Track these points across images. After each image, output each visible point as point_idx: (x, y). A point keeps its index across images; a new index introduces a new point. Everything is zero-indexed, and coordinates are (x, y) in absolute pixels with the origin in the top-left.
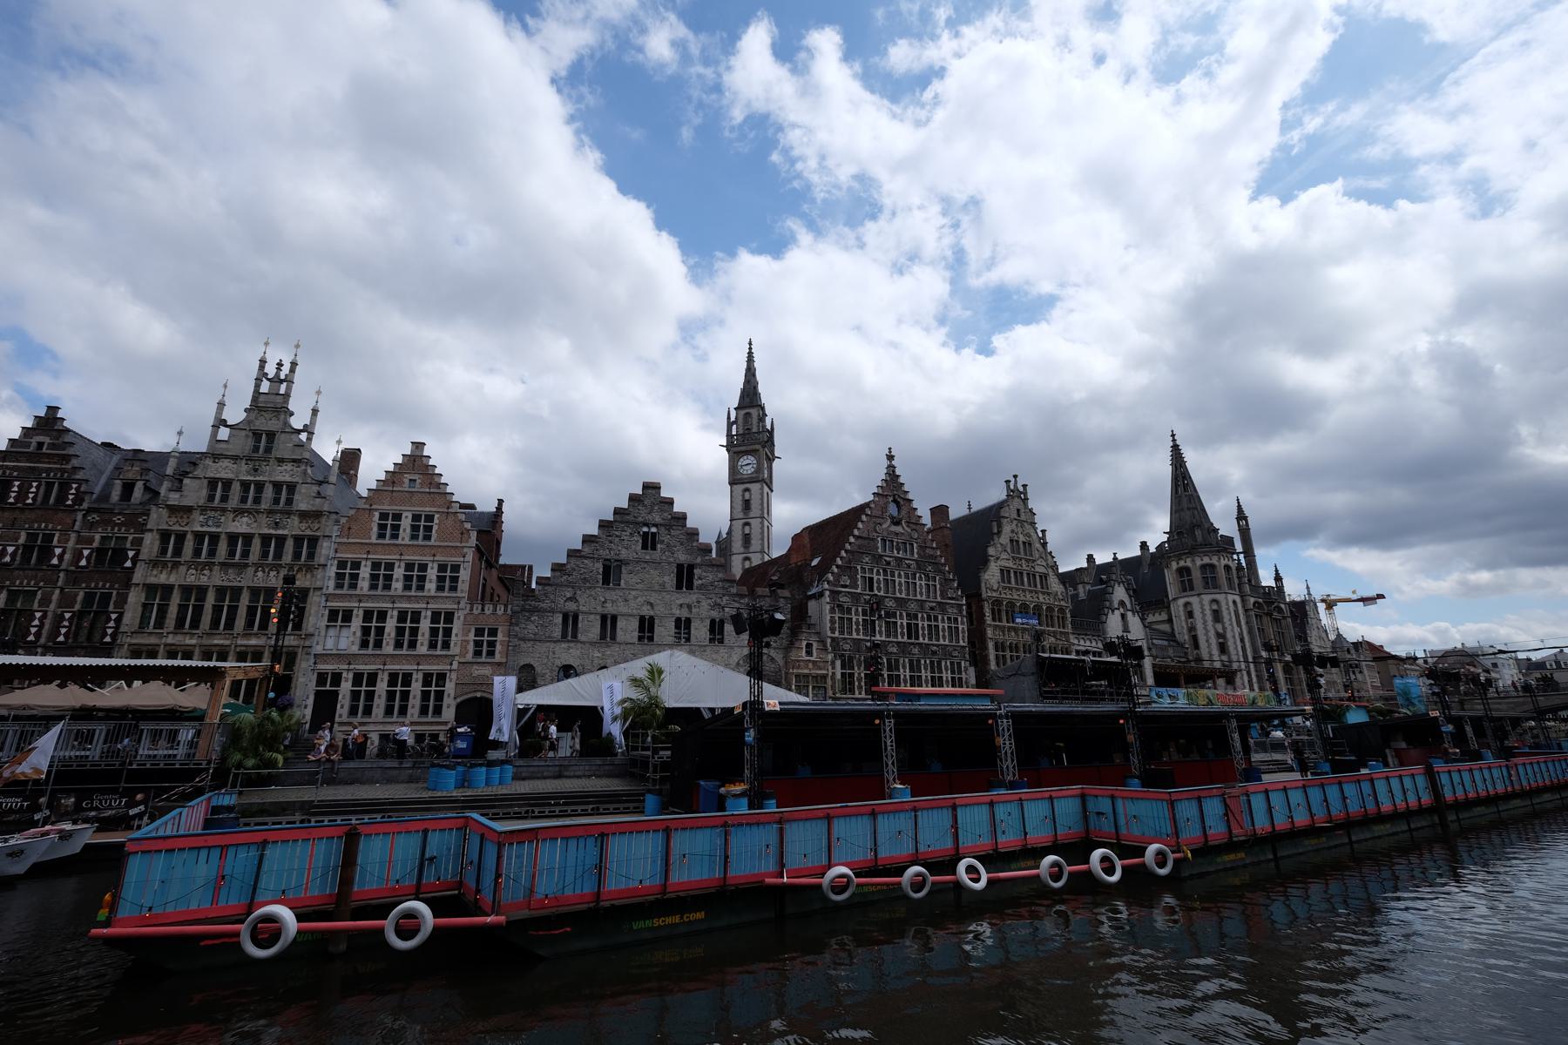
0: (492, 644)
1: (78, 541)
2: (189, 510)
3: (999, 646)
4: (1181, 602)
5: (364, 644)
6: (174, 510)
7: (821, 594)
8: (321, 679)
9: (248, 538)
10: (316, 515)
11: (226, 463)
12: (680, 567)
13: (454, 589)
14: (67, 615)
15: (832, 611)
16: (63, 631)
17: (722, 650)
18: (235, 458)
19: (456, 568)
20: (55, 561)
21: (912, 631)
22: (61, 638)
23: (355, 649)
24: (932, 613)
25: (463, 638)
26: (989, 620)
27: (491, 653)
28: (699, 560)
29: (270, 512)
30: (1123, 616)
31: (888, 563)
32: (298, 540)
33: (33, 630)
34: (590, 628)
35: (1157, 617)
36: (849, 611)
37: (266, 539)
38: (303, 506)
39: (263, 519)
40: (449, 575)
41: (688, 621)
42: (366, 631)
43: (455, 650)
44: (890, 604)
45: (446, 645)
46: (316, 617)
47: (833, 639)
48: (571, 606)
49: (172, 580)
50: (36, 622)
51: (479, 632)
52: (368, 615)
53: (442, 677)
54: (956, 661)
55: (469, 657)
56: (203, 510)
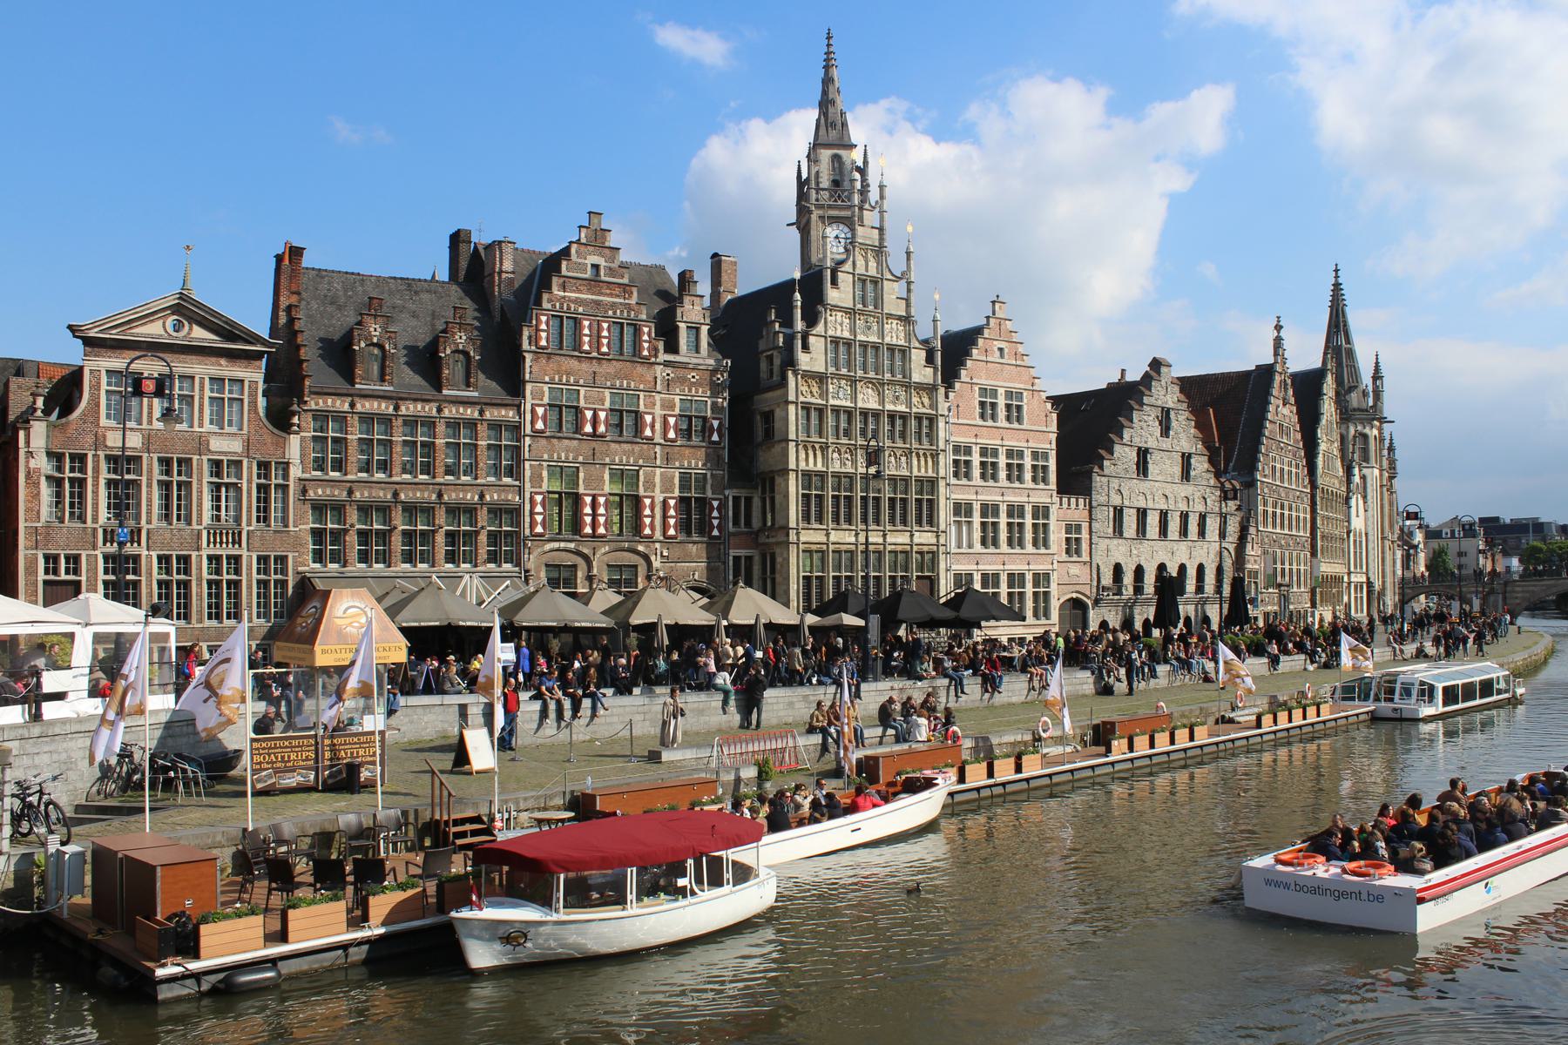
1: (663, 407)
2: (821, 378)
6: (808, 375)
9: (877, 415)
10: (931, 389)
13: (1045, 480)
14: (672, 502)
16: (672, 521)
19: (1046, 456)
20: (648, 432)
22: (672, 532)
25: (1057, 535)
27: (1078, 552)
29: (890, 382)
32: (919, 418)
33: (647, 521)
37: (892, 416)
38: (916, 378)
43: (1054, 548)
45: (1046, 545)
46: (944, 514)
49: (820, 467)
50: (647, 512)
53: (1047, 576)
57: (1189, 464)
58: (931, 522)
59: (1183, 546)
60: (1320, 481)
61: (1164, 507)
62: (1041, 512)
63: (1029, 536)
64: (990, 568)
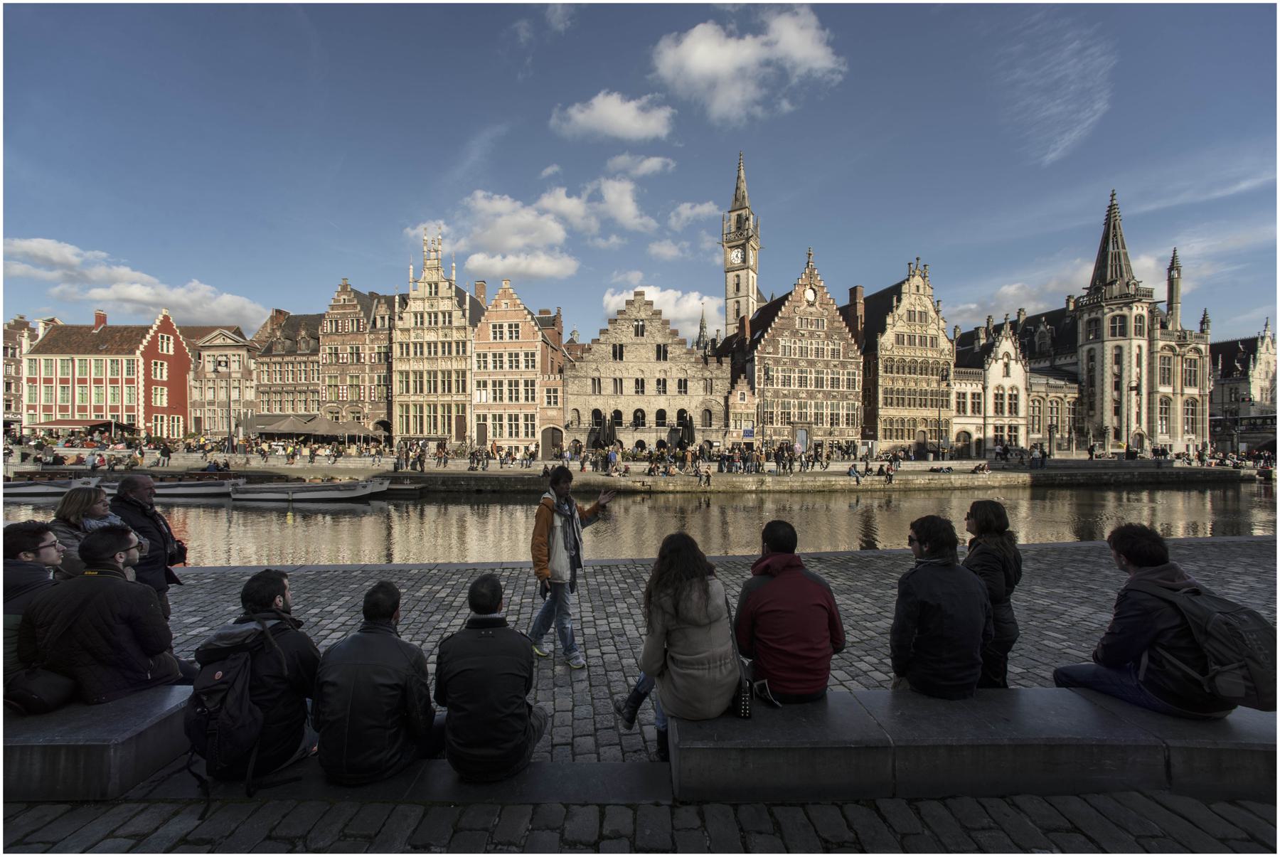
0: (556, 397)
2: (408, 330)
3: (885, 392)
4: (1086, 348)
5: (495, 399)
7: (753, 360)
8: (478, 416)
11: (419, 303)
12: (659, 346)
13: (533, 366)
15: (760, 370)
17: (686, 398)
18: (423, 299)
19: (533, 355)
21: (819, 382)
23: (491, 401)
25: (541, 394)
26: (881, 372)
27: (556, 403)
30: (1006, 365)
34: (608, 387)
35: (1069, 360)
37: (443, 343)
39: (440, 333)
40: (530, 356)
41: (665, 380)
42: (495, 392)
43: (537, 401)
44: (803, 364)
45: (533, 399)
48: (596, 374)
51: (549, 391)
52: (494, 384)
53: (533, 416)
55: (545, 405)
56: (416, 328)
57: (665, 352)
58: (464, 390)
59: (662, 398)
60: (882, 354)
61: (640, 376)
62: (530, 384)
63: (522, 395)
64: (497, 412)
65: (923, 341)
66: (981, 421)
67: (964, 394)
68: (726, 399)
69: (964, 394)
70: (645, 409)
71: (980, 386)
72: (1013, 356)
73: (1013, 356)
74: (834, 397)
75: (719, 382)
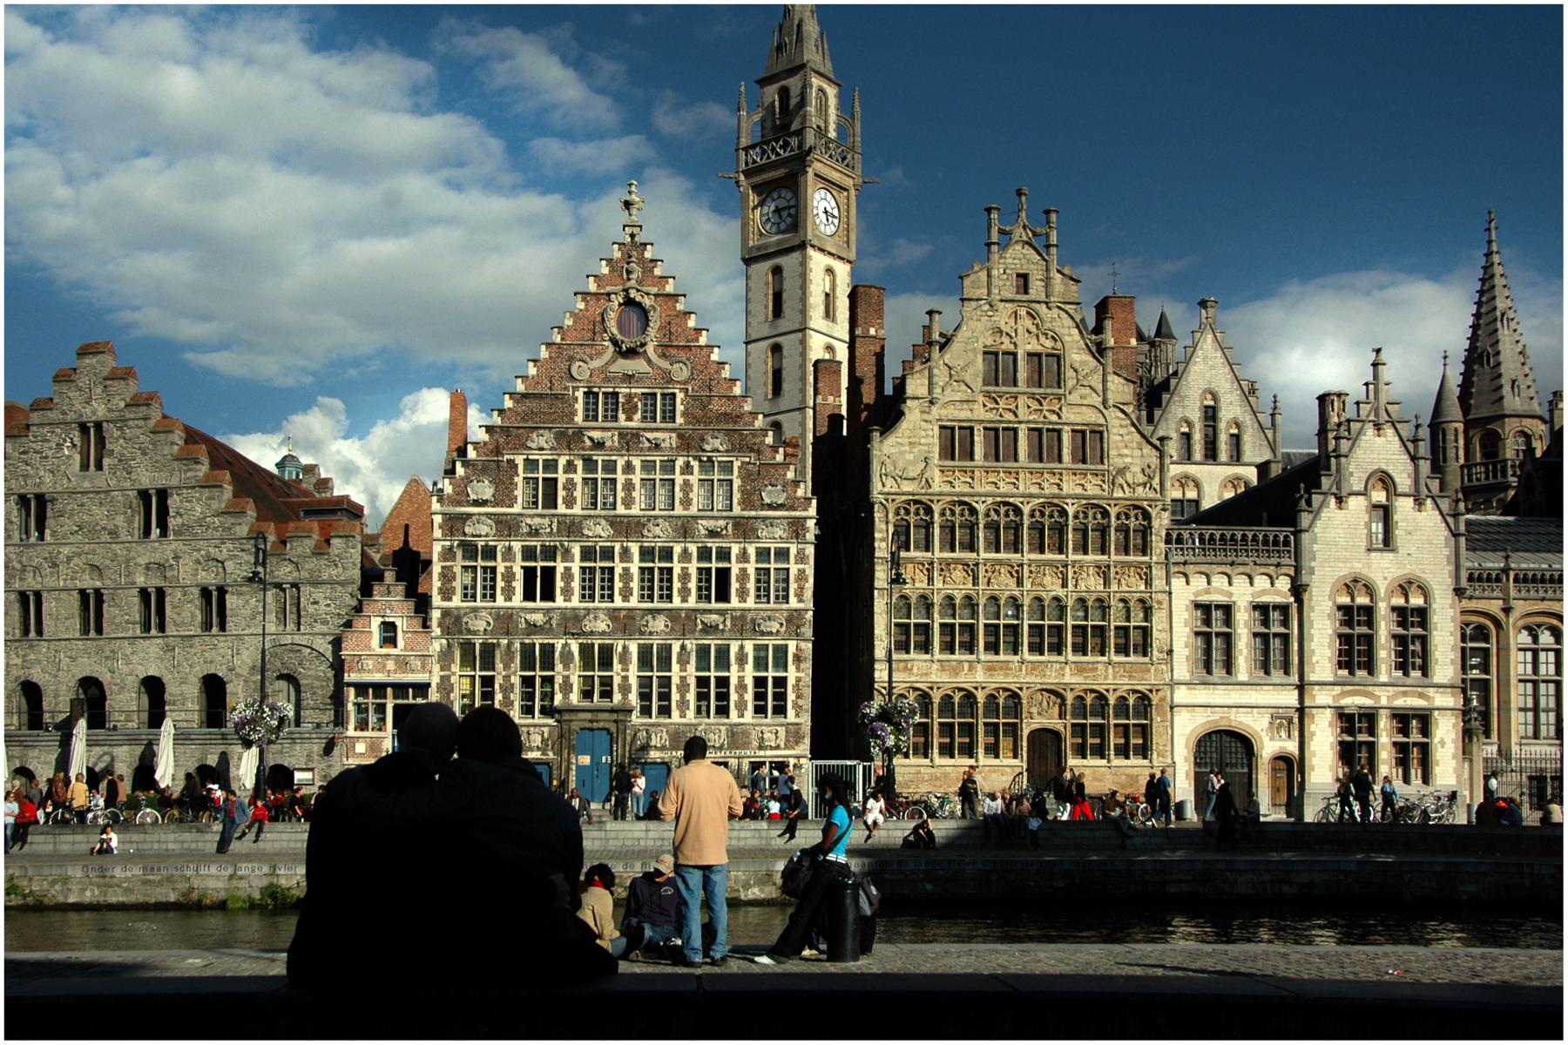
15: (448, 554)
21: (657, 582)
24: (714, 544)
28: (174, 481)
31: (599, 445)
36: (490, 553)
41: (161, 593)
44: (599, 531)
47: (446, 613)
54: (771, 642)
59: (153, 646)
61: (89, 582)
65: (1045, 443)
66: (1291, 698)
67: (1227, 610)
68: (337, 643)
69: (1227, 610)
70: (105, 677)
71: (1284, 584)
72: (1404, 481)
73: (1404, 481)
74: (709, 629)
75: (318, 594)
